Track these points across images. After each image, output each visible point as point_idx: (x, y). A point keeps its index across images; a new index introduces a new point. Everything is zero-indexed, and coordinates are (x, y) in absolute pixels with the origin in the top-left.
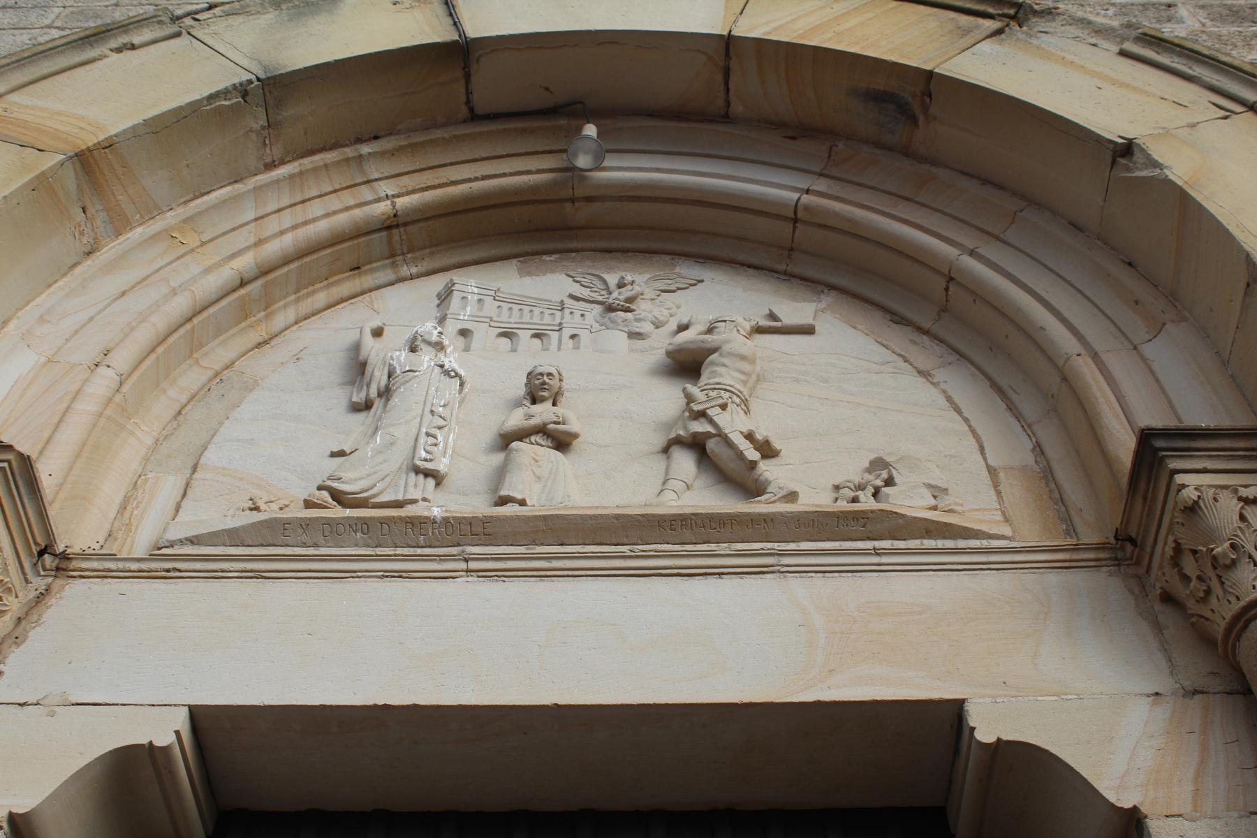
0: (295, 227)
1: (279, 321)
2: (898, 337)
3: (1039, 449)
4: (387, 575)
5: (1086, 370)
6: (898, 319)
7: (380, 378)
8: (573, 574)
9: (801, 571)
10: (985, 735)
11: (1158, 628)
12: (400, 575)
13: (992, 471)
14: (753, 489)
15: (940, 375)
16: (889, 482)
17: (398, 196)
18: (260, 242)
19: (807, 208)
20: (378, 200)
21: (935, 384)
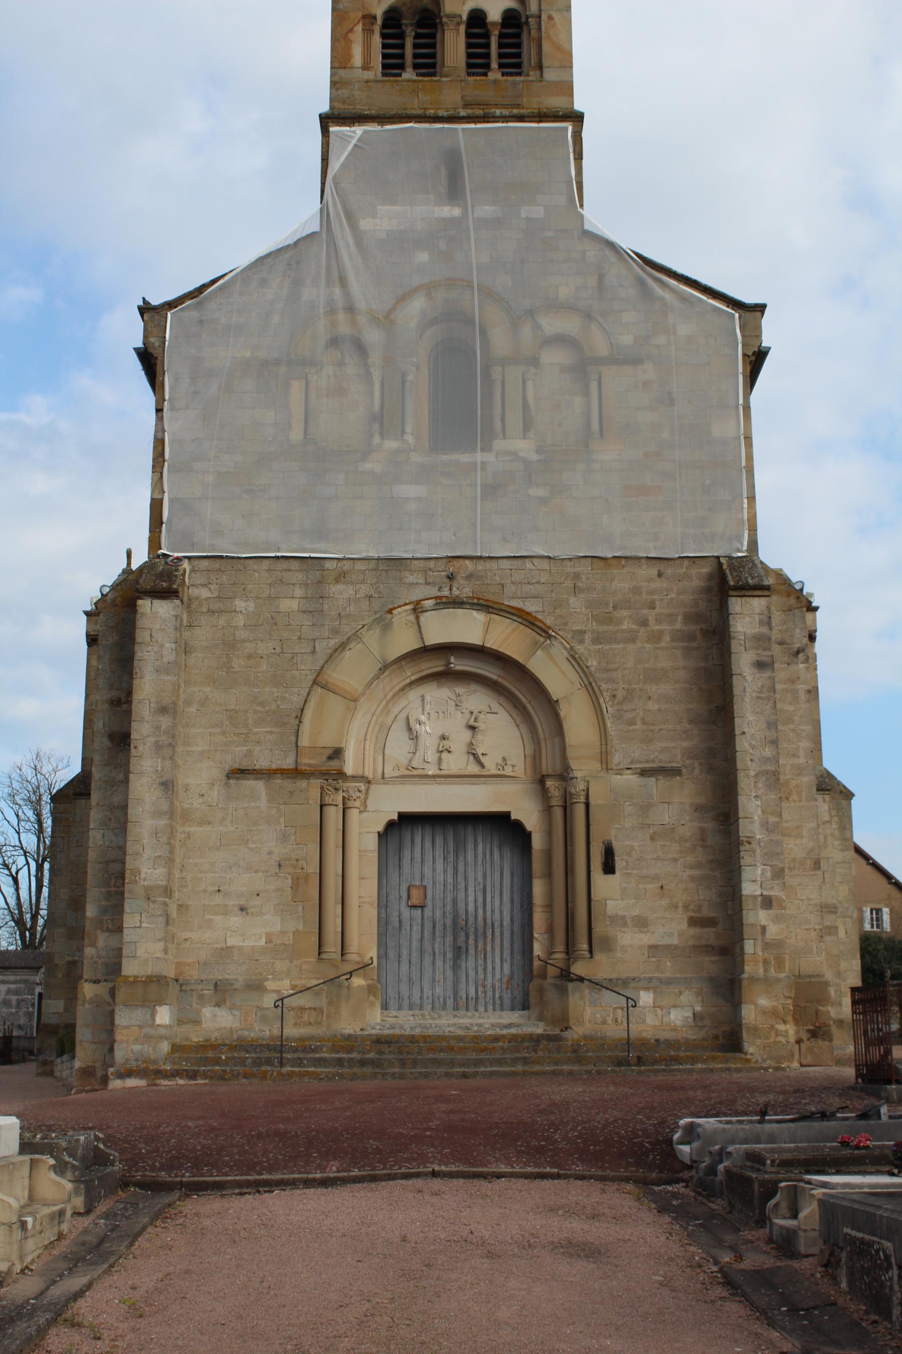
0: (391, 689)
1: (389, 706)
2: (514, 713)
3: (535, 750)
4: (423, 784)
5: (543, 743)
6: (515, 707)
7: (415, 734)
8: (453, 784)
9: (489, 784)
10: (513, 818)
11: (543, 797)
12: (425, 784)
13: (525, 756)
14: (483, 766)
15: (521, 726)
16: (506, 764)
17: (412, 675)
18: (386, 696)
19: (499, 682)
20: (407, 678)
21: (519, 729)
